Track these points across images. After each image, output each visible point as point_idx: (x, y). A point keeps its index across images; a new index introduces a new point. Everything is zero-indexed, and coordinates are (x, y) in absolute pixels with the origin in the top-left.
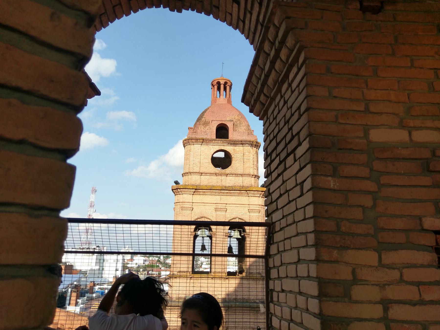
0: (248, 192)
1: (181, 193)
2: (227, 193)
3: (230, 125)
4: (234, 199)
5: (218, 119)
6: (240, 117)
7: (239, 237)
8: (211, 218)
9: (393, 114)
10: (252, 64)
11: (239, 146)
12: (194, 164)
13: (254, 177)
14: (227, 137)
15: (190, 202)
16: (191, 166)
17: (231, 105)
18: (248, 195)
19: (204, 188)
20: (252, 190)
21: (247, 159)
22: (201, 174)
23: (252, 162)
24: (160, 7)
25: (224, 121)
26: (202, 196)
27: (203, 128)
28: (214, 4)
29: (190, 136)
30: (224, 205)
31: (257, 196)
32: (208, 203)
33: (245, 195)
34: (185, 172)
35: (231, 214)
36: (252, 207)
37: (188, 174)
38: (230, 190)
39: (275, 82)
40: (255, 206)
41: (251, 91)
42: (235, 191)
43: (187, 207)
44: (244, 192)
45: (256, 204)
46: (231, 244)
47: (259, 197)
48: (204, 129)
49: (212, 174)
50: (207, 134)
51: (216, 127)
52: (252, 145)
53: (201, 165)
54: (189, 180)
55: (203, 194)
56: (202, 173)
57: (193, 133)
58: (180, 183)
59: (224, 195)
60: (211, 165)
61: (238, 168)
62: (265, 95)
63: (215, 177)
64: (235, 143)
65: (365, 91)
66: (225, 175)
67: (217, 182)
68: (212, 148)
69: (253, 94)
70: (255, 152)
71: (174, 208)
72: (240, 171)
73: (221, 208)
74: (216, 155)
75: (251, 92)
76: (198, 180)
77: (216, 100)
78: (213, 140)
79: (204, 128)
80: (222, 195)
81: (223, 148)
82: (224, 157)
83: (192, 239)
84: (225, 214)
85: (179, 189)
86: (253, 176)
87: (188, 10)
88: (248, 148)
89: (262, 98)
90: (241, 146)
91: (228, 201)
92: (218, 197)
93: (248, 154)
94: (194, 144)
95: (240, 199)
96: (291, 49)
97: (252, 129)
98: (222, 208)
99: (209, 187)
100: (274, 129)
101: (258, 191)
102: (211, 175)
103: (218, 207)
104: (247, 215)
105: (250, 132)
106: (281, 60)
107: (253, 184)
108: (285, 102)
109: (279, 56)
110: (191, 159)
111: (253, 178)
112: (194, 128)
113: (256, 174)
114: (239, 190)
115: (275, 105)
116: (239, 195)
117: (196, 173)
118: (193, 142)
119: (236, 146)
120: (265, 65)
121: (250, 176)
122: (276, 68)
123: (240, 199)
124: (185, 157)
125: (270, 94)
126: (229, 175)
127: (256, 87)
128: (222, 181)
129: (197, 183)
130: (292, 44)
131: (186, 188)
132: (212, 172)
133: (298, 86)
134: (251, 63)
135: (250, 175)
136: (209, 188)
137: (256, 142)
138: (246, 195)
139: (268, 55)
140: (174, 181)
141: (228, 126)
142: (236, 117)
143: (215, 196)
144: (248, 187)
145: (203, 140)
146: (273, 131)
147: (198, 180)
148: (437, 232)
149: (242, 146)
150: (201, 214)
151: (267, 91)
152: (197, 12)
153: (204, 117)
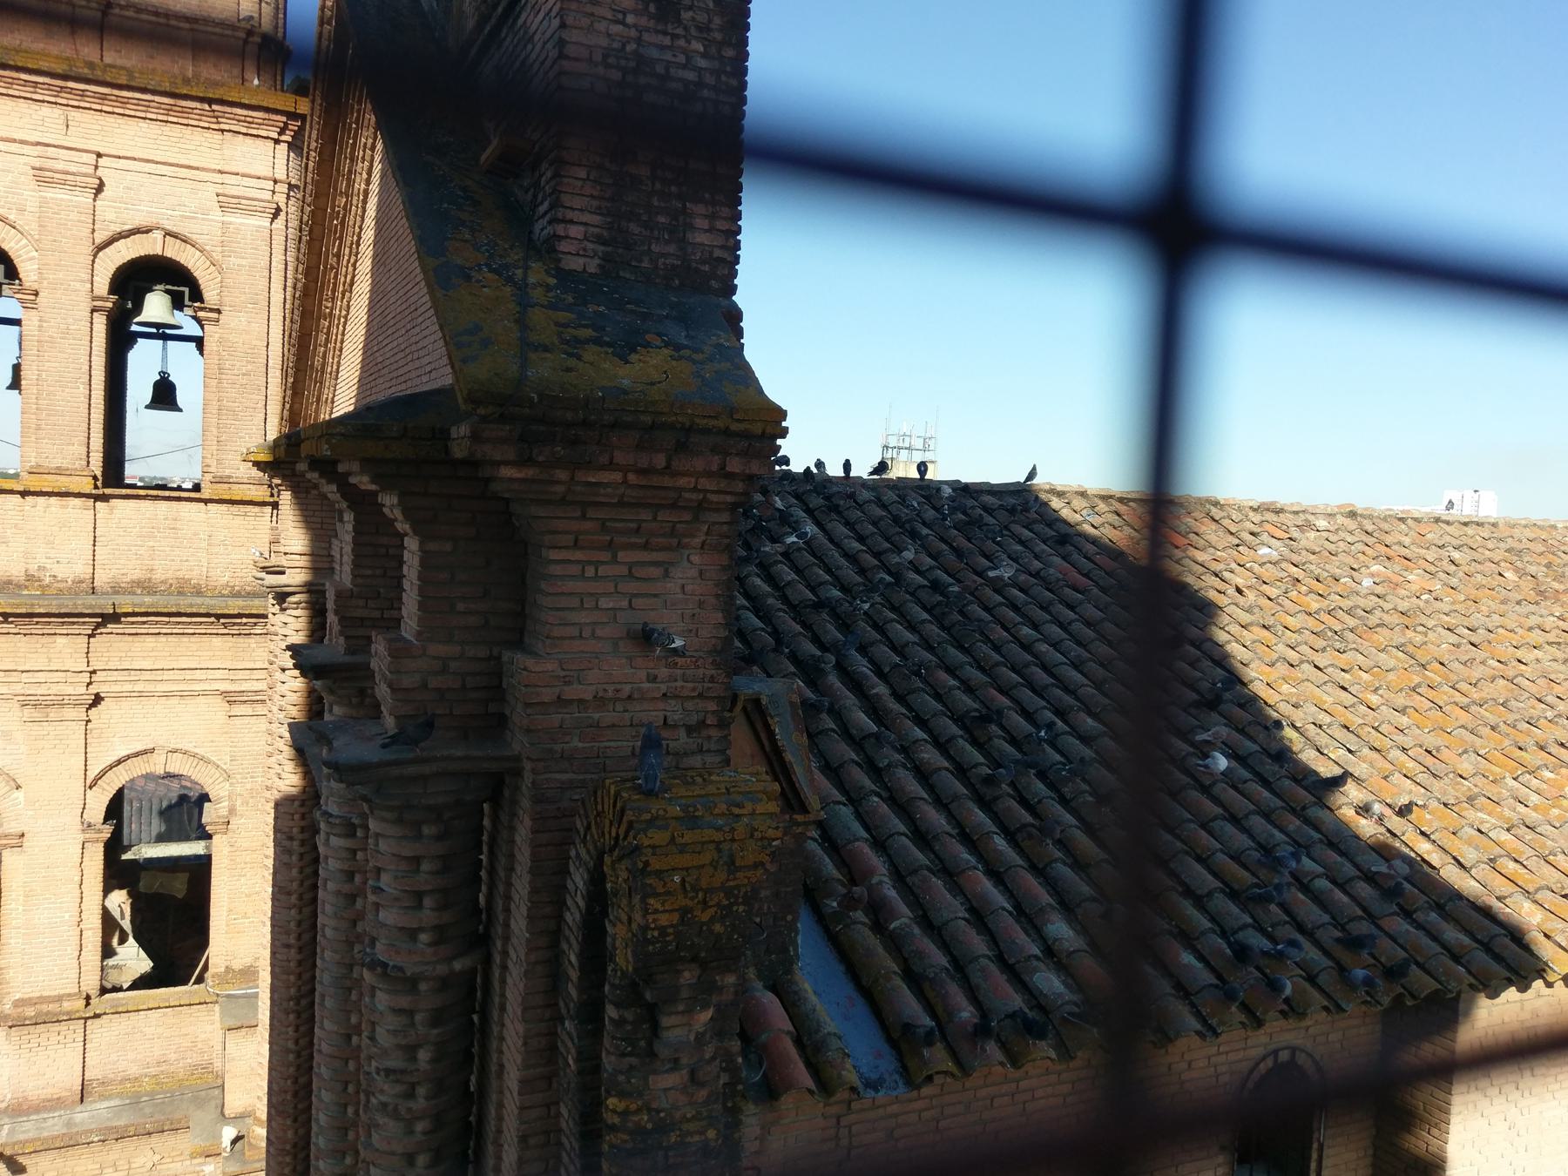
8: (12, 217)
40: (254, 182)
44: (198, 105)
45: (259, 174)
59: (88, 105)
73: (67, 173)
84: (87, 203)
92: (50, 110)
95: (178, 140)
98: (73, 168)
114: (168, 89)
116: (171, 119)
138: (206, 125)
143: (35, 106)
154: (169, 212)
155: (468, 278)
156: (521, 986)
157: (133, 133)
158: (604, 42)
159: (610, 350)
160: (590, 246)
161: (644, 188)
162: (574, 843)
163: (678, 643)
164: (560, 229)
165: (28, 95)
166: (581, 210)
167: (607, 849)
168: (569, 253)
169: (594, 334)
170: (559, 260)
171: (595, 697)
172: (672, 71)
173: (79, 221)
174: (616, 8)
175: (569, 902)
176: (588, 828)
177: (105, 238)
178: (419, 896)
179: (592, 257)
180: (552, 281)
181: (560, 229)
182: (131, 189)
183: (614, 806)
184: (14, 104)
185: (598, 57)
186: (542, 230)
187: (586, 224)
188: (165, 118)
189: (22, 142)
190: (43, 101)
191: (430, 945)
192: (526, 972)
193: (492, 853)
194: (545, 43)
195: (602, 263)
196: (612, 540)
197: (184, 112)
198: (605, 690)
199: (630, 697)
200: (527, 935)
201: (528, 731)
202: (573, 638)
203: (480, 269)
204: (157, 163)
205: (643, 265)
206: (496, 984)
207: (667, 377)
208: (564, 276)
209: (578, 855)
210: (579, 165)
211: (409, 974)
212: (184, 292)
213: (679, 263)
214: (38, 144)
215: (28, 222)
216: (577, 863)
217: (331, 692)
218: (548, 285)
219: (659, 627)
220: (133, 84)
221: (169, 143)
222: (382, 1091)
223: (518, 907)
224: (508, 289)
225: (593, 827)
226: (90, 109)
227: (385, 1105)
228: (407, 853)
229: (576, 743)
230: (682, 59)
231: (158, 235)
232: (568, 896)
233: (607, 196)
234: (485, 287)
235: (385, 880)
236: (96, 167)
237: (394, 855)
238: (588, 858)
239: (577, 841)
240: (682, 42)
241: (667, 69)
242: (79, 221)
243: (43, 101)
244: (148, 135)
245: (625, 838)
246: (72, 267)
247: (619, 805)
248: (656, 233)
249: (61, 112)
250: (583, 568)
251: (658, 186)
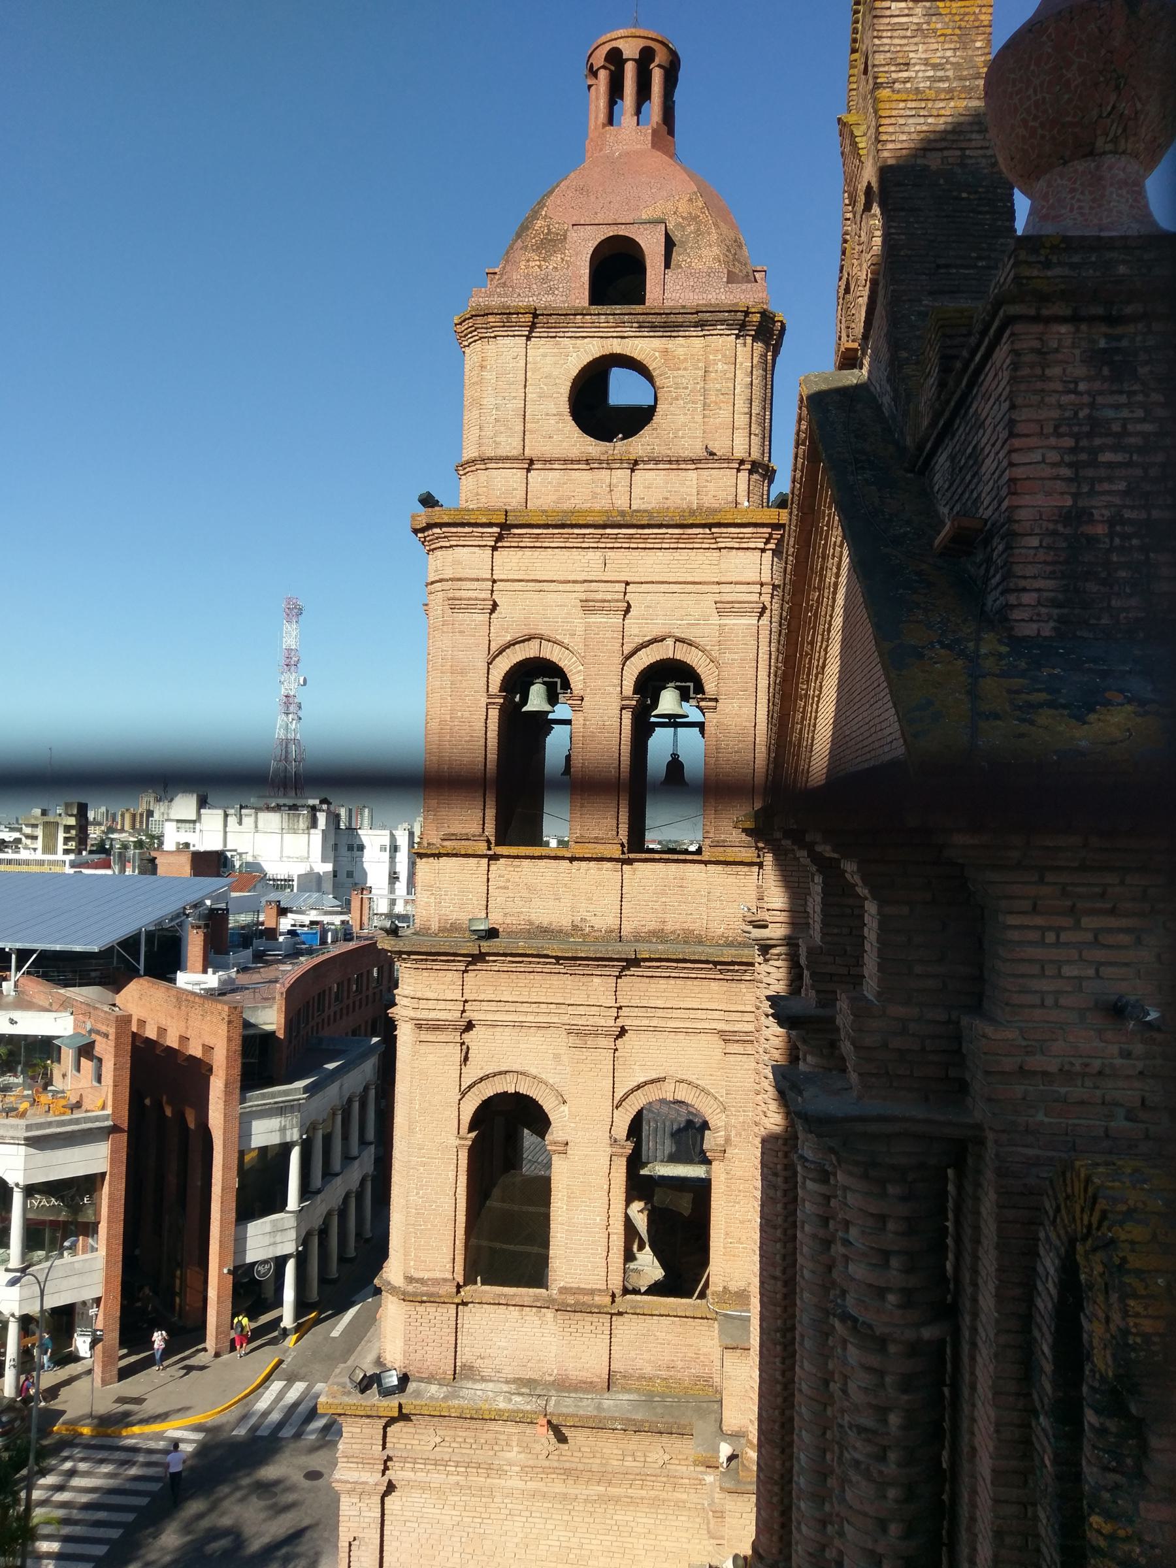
0: (714, 530)
2: (631, 537)
4: (658, 562)
8: (566, 641)
13: (749, 467)
18: (714, 546)
19: (535, 518)
20: (730, 521)
26: (528, 552)
30: (617, 589)
31: (752, 545)
33: (704, 546)
45: (748, 580)
49: (572, 462)
55: (532, 545)
59: (619, 545)
66: (625, 465)
67: (595, 495)
73: (605, 601)
76: (517, 490)
86: (742, 467)
91: (633, 570)
95: (684, 562)
98: (609, 597)
101: (755, 525)
102: (570, 466)
104: (708, 624)
123: (684, 562)
132: (574, 453)
135: (729, 460)
138: (707, 546)
143: (583, 552)
154: (679, 622)
155: (921, 656)
156: (991, 1368)
157: (652, 562)
158: (1055, 414)
159: (1066, 712)
160: (1043, 610)
161: (1101, 546)
162: (1042, 1224)
163: (1153, 1015)
164: (1012, 599)
165: (579, 545)
166: (1035, 577)
167: (1079, 1236)
168: (1023, 620)
169: (1049, 697)
170: (1012, 628)
171: (1061, 1070)
172: (1130, 427)
173: (612, 638)
174: (1068, 379)
175: (1040, 1288)
176: (1058, 1210)
177: (631, 649)
178: (886, 1255)
179: (1047, 622)
180: (1004, 649)
181: (1012, 599)
183: (1086, 1191)
185: (1048, 429)
186: (995, 601)
187: (1038, 590)
188: (675, 546)
189: (575, 582)
190: (589, 548)
191: (899, 1307)
192: (996, 1355)
193: (958, 1223)
194: (995, 427)
195: (1058, 625)
196: (1074, 905)
197: (690, 538)
198: (1072, 1064)
199: (1100, 1073)
200: (996, 1315)
201: (990, 1100)
202: (1033, 1006)
203: (934, 647)
204: (670, 583)
205: (1103, 621)
206: (966, 1360)
207: (1131, 735)
208: (1017, 643)
209: (1048, 1238)
210: (1031, 535)
211: (878, 1333)
213: (1143, 615)
214: (585, 581)
215: (576, 644)
216: (1047, 1247)
217: (805, 1041)
218: (1000, 654)
219: (1132, 998)
220: (653, 522)
221: (679, 566)
222: (855, 1448)
223: (986, 1283)
224: (960, 662)
225: (1063, 1212)
226: (621, 548)
227: (857, 1463)
228: (873, 1210)
229: (1041, 1117)
230: (1140, 413)
231: (670, 642)
232: (1039, 1283)
233: (1061, 559)
234: (936, 663)
235: (854, 1233)
236: (625, 593)
237: (861, 1210)
238: (1058, 1243)
239: (1047, 1223)
240: (1140, 398)
241: (1124, 426)
242: (612, 638)
243: (589, 548)
244: (664, 562)
245: (1098, 1229)
246: (607, 675)
247: (1090, 1190)
248: (1116, 588)
249: (600, 554)
250: (1043, 934)
251: (1117, 541)
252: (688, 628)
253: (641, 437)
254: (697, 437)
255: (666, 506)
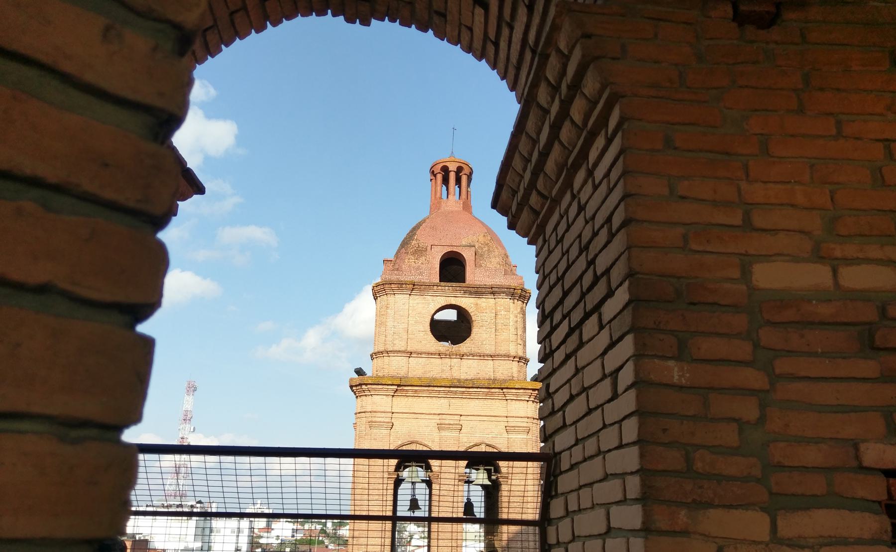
0: (504, 390)
1: (369, 394)
2: (463, 393)
3: (468, 255)
4: (476, 405)
5: (443, 242)
6: (489, 238)
7: (487, 482)
9: (802, 232)
10: (512, 130)
11: (487, 297)
12: (394, 333)
13: (518, 360)
14: (463, 280)
15: (387, 412)
16: (389, 338)
17: (471, 213)
18: (504, 398)
20: (512, 387)
21: (503, 323)
22: (409, 355)
23: (512, 330)
24: (326, 14)
25: (455, 247)
26: (410, 399)
27: (414, 260)
28: (435, 8)
29: (387, 276)
30: (456, 418)
32: (424, 414)
33: (499, 398)
34: (376, 351)
35: (471, 436)
36: (513, 422)
37: (384, 355)
38: (469, 388)
39: (561, 167)
40: (519, 420)
41: (512, 186)
42: (479, 390)
43: (380, 422)
44: (497, 390)
45: (522, 416)
46: (471, 498)
47: (528, 401)
48: (414, 262)
49: (432, 354)
50: (421, 274)
51: (440, 258)
52: (512, 295)
53: (410, 336)
54: (385, 367)
55: (413, 395)
56: (411, 353)
57: (392, 270)
58: (366, 373)
59: (457, 396)
60: (430, 337)
61: (484, 343)
62: (540, 193)
63: (437, 361)
64: (478, 292)
65: (744, 185)
66: (458, 357)
67: (443, 371)
68: (431, 301)
69: (515, 192)
70: (519, 310)
71: (354, 424)
72: (489, 349)
73: (450, 424)
74: (440, 316)
75: (510, 187)
76: (403, 367)
77: (439, 203)
78: (434, 286)
79: (416, 260)
80: (451, 396)
81: (453, 301)
82: (456, 319)
83: (392, 486)
85: (364, 384)
86: (515, 359)
87: (383, 20)
88: (504, 302)
89: (534, 199)
90: (490, 297)
91: (464, 409)
93: (506, 313)
94: (394, 294)
95: (490, 405)
96: (593, 100)
97: (513, 263)
98: (452, 423)
99: (425, 381)
100: (559, 262)
102: (430, 356)
103: (443, 422)
104: (502, 437)
105: (509, 269)
106: (573, 122)
107: (515, 375)
108: (581, 208)
109: (569, 115)
110: (390, 324)
111: (516, 363)
112: (396, 261)
113: (521, 354)
114: (487, 386)
115: (560, 214)
117: (399, 351)
118: (393, 290)
119: (480, 297)
120: (539, 133)
121: (510, 359)
122: (561, 139)
123: (490, 405)
124: (376, 320)
125: (550, 192)
126: (466, 357)
127: (522, 177)
128: (451, 369)
129: (402, 372)
130: (594, 90)
131: (378, 382)
132: (432, 350)
133: (607, 175)
134: (511, 129)
135: (509, 356)
136: (426, 383)
137: (522, 290)
138: (501, 398)
139: (546, 112)
140: (355, 369)
141: (464, 256)
142: (481, 239)
143: (438, 399)
144: (505, 381)
145: (414, 285)
146: (556, 266)
147: (403, 367)
148: (890, 473)
149: (493, 297)
150: (409, 436)
151: (544, 186)
152: (401, 24)
153: (416, 238)
154: (487, 436)
173: (454, 443)
182: (472, 428)
184: (430, 400)
189: (434, 414)
197: (492, 393)
212: (491, 469)
220: (474, 386)
252: (492, 439)
253: (465, 344)
254: (492, 345)
255: (478, 377)
